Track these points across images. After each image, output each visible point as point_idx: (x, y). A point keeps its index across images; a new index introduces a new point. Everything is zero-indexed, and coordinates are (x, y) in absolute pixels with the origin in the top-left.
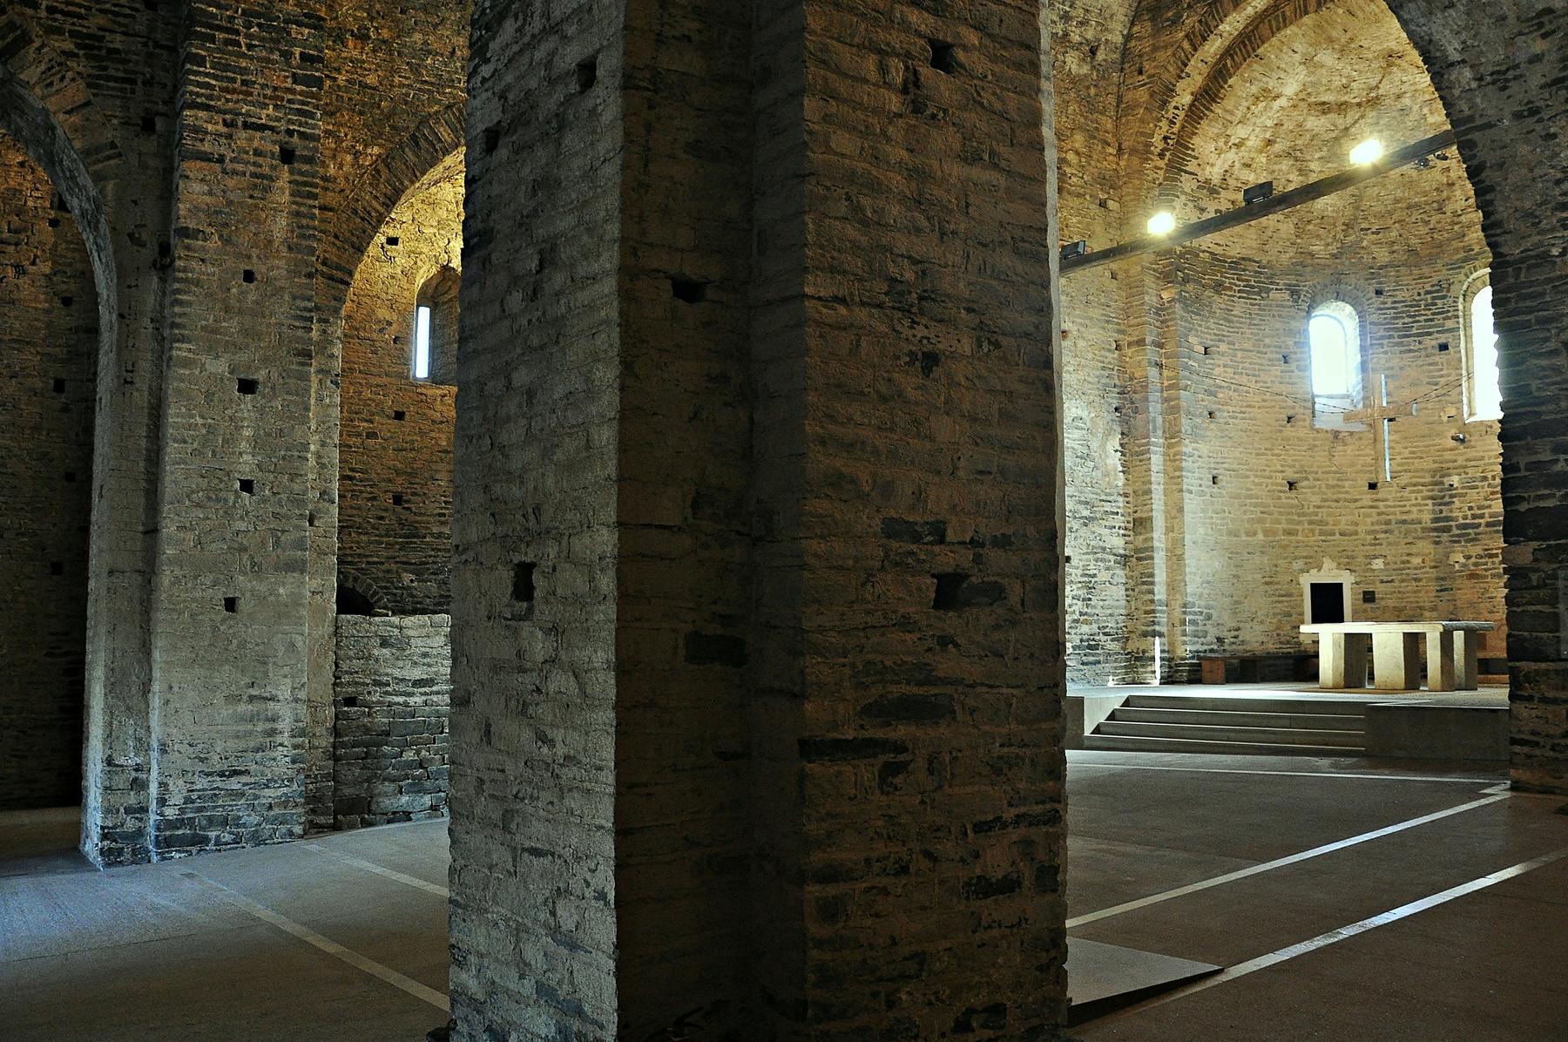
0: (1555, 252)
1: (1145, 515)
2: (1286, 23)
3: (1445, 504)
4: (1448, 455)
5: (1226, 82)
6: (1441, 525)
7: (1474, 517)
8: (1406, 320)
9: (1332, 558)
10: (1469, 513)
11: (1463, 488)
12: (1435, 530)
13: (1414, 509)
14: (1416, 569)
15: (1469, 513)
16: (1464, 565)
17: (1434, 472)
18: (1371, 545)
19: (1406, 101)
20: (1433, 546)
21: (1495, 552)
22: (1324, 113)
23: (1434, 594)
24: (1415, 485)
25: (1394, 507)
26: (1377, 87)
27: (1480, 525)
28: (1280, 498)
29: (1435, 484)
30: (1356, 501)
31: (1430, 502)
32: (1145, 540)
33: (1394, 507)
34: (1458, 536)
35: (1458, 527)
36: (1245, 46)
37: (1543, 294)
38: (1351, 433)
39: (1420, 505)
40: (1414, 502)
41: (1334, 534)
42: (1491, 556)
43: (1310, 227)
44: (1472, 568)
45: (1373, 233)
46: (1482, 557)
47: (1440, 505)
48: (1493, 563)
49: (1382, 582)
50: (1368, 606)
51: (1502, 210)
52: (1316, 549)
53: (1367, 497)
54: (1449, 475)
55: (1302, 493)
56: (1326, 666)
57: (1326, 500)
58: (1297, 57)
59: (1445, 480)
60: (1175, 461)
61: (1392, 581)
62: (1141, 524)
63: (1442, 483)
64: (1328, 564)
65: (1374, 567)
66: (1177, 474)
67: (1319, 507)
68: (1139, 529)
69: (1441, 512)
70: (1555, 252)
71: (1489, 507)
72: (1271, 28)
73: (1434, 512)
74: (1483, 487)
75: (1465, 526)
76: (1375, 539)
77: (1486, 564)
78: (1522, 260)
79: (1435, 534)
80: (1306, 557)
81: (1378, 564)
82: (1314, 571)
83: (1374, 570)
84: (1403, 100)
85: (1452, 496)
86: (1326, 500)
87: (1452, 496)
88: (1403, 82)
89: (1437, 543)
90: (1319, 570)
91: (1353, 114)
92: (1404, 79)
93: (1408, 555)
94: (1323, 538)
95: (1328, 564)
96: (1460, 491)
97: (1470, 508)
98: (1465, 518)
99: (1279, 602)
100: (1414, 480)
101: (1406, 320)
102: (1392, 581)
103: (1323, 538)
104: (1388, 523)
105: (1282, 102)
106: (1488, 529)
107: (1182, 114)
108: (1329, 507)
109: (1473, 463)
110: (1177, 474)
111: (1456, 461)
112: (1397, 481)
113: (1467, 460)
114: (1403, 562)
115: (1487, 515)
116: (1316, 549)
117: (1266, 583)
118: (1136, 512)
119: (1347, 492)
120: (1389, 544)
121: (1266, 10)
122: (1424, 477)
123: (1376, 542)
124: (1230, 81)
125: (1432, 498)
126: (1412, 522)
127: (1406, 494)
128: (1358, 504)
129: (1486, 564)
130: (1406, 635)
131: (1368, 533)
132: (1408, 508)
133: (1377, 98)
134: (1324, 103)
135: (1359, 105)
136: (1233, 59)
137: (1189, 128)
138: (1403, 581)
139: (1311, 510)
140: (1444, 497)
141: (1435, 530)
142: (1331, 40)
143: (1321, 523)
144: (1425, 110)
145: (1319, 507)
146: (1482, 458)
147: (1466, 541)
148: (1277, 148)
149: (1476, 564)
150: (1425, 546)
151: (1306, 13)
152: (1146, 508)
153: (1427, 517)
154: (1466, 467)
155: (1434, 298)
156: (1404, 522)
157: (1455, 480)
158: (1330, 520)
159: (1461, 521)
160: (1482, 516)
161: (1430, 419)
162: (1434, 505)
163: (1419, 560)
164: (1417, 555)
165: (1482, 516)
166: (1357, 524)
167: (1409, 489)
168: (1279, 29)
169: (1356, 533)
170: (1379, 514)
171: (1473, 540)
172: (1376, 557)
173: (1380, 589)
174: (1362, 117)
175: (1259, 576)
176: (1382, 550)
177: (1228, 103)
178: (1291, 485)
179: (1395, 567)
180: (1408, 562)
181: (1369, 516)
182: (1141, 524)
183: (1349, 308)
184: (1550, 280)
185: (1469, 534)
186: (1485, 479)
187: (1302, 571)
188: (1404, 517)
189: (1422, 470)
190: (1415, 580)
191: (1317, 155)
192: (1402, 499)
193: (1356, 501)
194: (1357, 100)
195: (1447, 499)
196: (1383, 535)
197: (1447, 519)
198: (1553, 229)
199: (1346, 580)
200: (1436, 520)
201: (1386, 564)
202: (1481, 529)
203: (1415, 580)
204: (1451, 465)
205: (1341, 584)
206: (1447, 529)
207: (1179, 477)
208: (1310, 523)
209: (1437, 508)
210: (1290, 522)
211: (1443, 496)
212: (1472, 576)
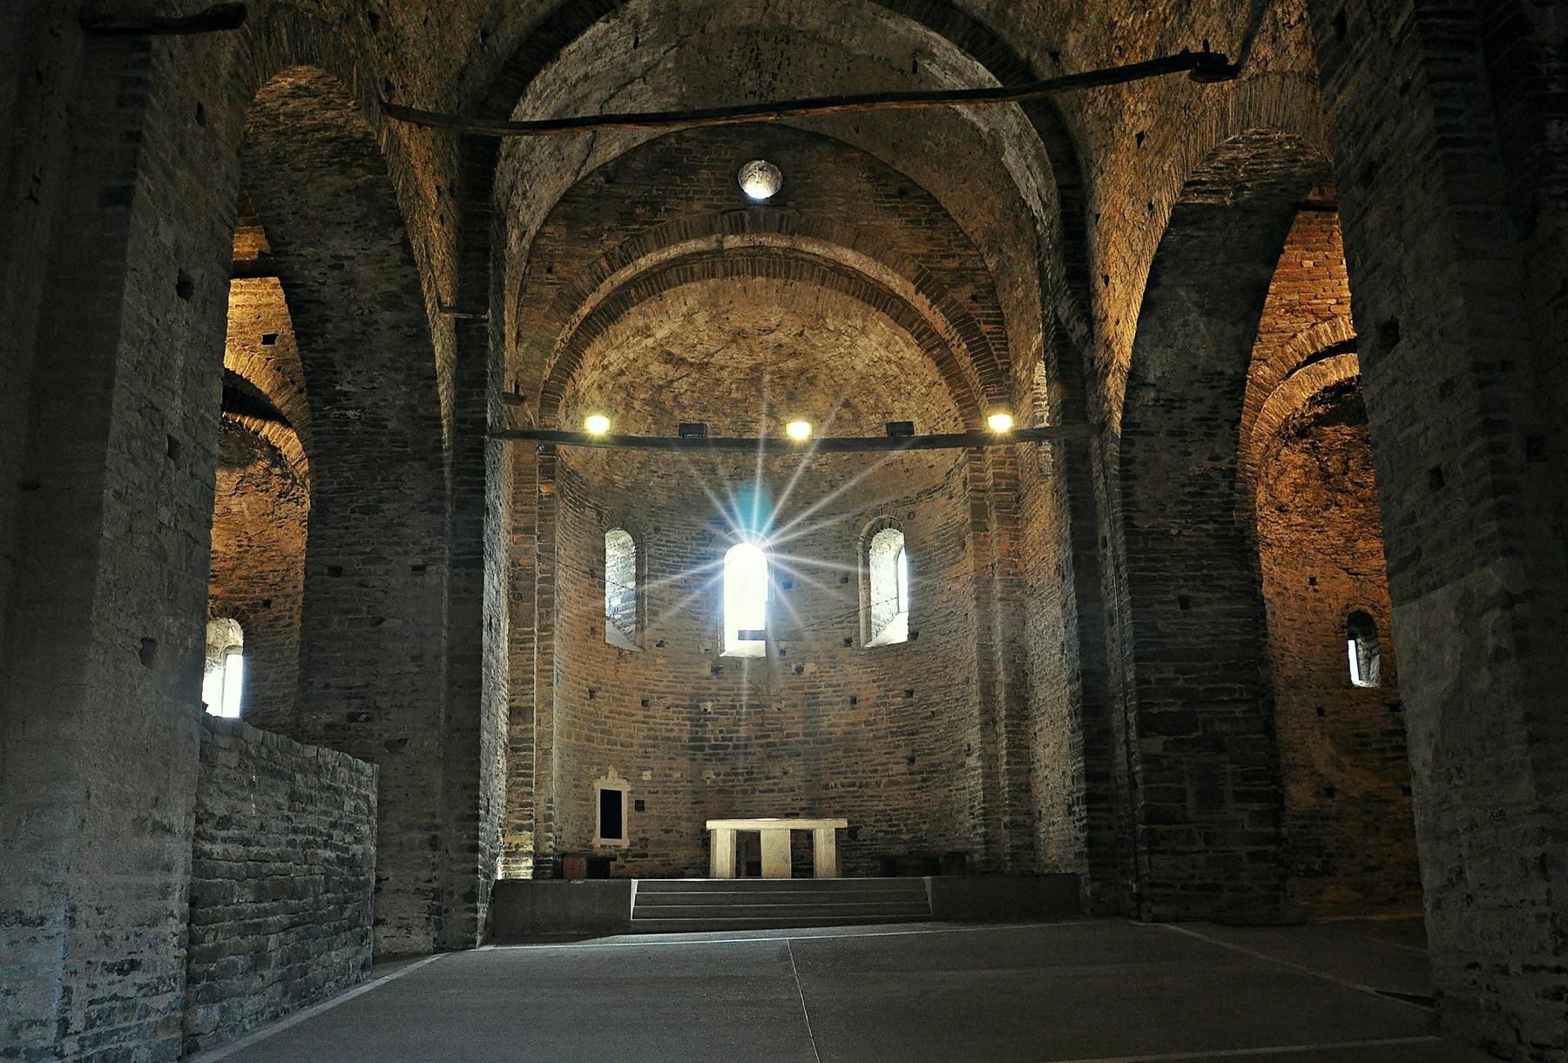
0: (1173, 532)
1: (523, 705)
2: (692, 277)
3: (701, 726)
4: (704, 683)
5: (627, 309)
6: (697, 744)
7: (724, 739)
8: (676, 559)
9: (616, 767)
10: (720, 736)
11: (715, 713)
12: (692, 748)
13: (676, 728)
14: (676, 782)
15: (720, 736)
16: (714, 782)
17: (692, 697)
18: (642, 757)
19: (725, 374)
20: (687, 762)
22: (666, 362)
23: (689, 805)
26: (712, 356)
27: (728, 747)
28: (584, 705)
29: (692, 707)
30: (633, 715)
31: (688, 723)
32: (522, 731)
33: (661, 724)
34: (709, 755)
35: (710, 747)
36: (651, 284)
37: (1164, 560)
38: (631, 652)
39: (678, 724)
40: (676, 722)
43: (617, 458)
44: (721, 784)
45: (659, 477)
46: (729, 775)
49: (649, 792)
51: (1139, 495)
52: (605, 757)
53: (640, 714)
54: (704, 701)
55: (597, 702)
56: (724, 859)
58: (684, 309)
59: (701, 704)
60: (545, 654)
62: (520, 713)
63: (698, 707)
64: (612, 772)
65: (644, 778)
66: (548, 667)
67: (608, 717)
68: (517, 719)
69: (697, 733)
70: (1173, 532)
72: (679, 277)
73: (691, 732)
75: (716, 747)
76: (646, 752)
78: (1150, 533)
81: (647, 776)
83: (643, 781)
84: (722, 372)
85: (706, 720)
87: (706, 720)
88: (732, 358)
89: (693, 760)
91: (683, 371)
92: (735, 356)
95: (612, 772)
96: (712, 716)
97: (721, 732)
101: (676, 559)
102: (657, 792)
104: (656, 738)
105: (650, 342)
107: (578, 322)
108: (614, 718)
110: (548, 667)
114: (666, 776)
116: (605, 757)
117: (576, 786)
118: (513, 701)
119: (626, 706)
120: (656, 758)
121: (672, 260)
122: (684, 701)
123: (646, 756)
124: (632, 310)
125: (690, 719)
126: (675, 739)
127: (670, 714)
128: (634, 718)
130: (795, 833)
131: (641, 746)
133: (707, 364)
134: (670, 354)
135: (692, 364)
136: (637, 290)
137: (583, 338)
138: (665, 793)
139: (603, 719)
141: (692, 748)
142: (715, 305)
143: (609, 732)
144: (734, 386)
145: (608, 717)
147: (719, 760)
148: (624, 380)
149: (723, 781)
150: (684, 762)
151: (714, 276)
152: (524, 698)
153: (686, 736)
155: (698, 545)
156: (668, 739)
157: (709, 705)
158: (614, 731)
160: (731, 739)
161: (692, 650)
162: (692, 726)
163: (678, 775)
164: (677, 769)
165: (731, 739)
166: (632, 738)
168: (686, 281)
170: (650, 729)
171: (723, 759)
173: (648, 799)
174: (687, 375)
176: (651, 762)
177: (620, 327)
178: (592, 693)
179: (660, 779)
180: (670, 776)
181: (640, 730)
182: (520, 713)
183: (626, 537)
184: (1168, 551)
185: (719, 754)
189: (683, 694)
190: (676, 792)
191: (642, 396)
192: (667, 718)
194: (693, 360)
196: (651, 750)
198: (1175, 517)
199: (624, 788)
200: (693, 739)
202: (729, 750)
203: (676, 792)
204: (705, 692)
205: (620, 792)
206: (701, 748)
207: (549, 671)
208: (602, 732)
210: (590, 729)
211: (698, 719)
212: (720, 791)
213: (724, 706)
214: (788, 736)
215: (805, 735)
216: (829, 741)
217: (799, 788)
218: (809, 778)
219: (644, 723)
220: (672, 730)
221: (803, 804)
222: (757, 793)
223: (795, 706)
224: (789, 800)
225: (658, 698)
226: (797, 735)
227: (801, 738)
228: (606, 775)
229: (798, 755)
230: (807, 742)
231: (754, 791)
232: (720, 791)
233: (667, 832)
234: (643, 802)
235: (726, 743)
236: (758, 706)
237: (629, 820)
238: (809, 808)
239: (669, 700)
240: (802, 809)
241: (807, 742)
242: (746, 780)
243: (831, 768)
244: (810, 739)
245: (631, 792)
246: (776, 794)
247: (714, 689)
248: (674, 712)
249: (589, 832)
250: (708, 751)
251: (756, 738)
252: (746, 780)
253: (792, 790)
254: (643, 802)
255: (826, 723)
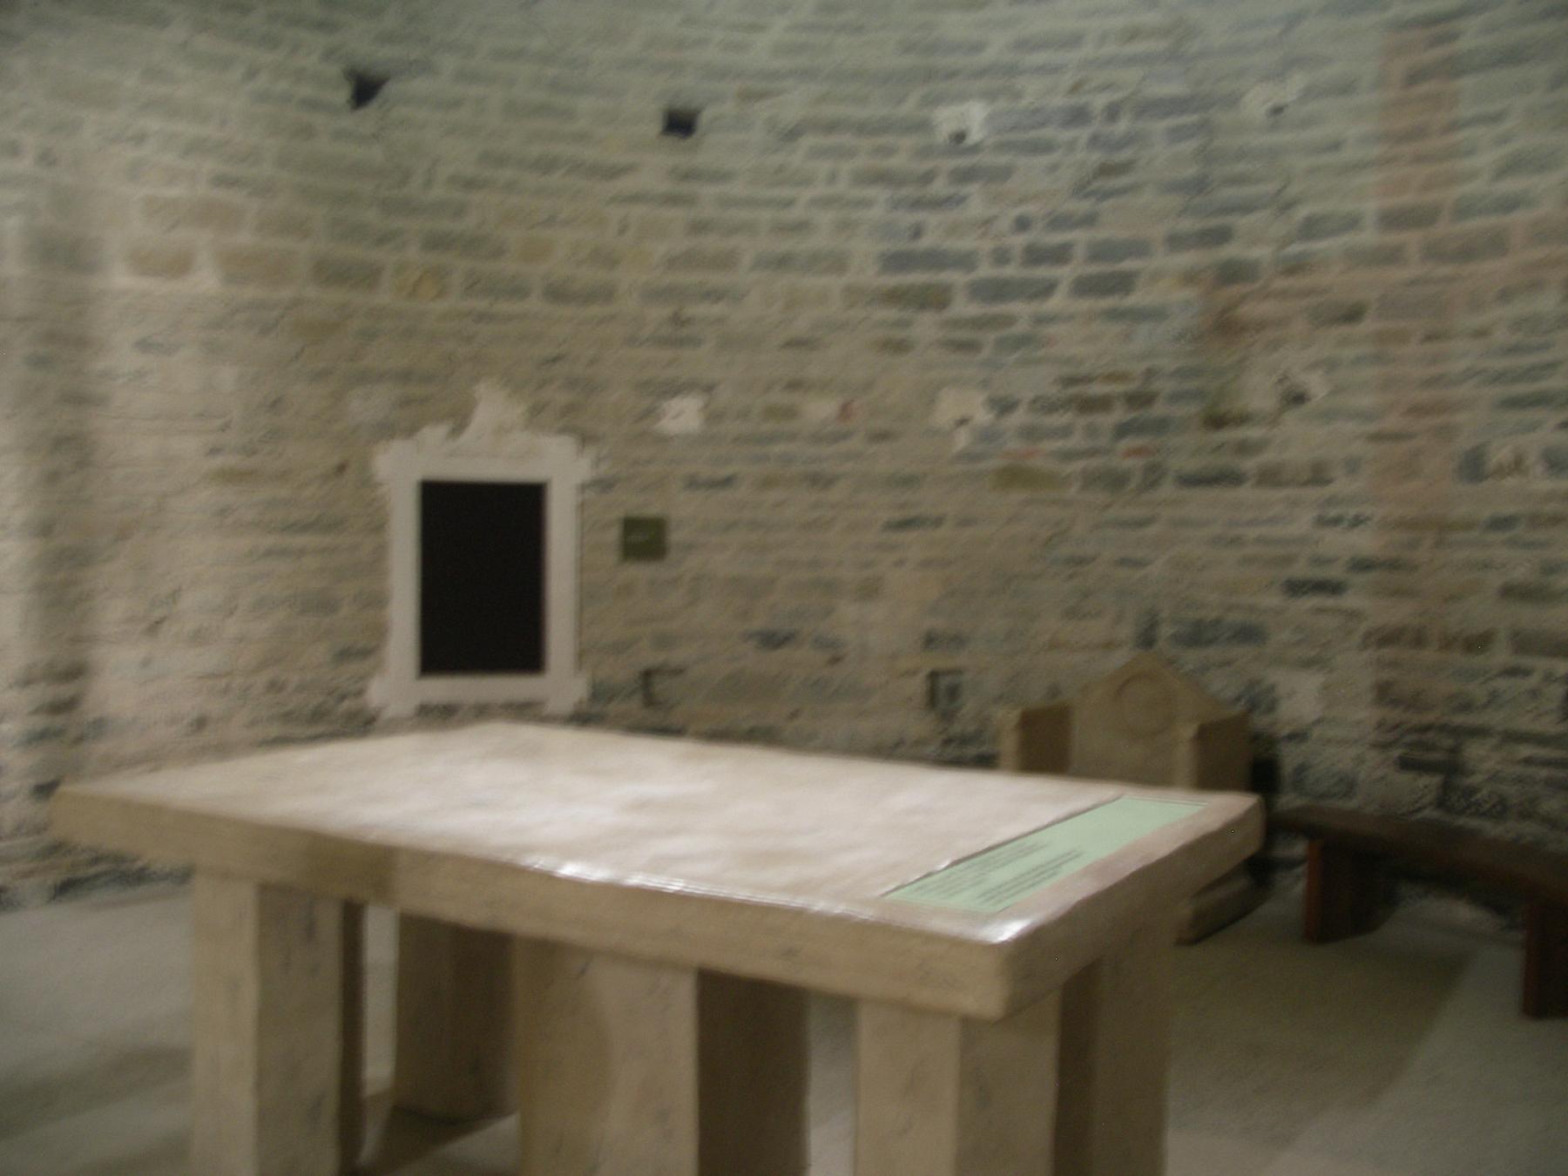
3: (938, 204)
7: (1035, 256)
11: (1003, 147)
12: (894, 297)
13: (825, 218)
14: (817, 438)
15: (1019, 241)
21: (1097, 389)
24: (832, 127)
25: (751, 203)
30: (613, 173)
33: (751, 203)
40: (820, 190)
41: (518, 291)
42: (1089, 405)
47: (917, 204)
48: (1091, 431)
49: (693, 483)
50: (640, 572)
54: (961, 97)
57: (501, 161)
61: (727, 482)
63: (923, 126)
69: (917, 232)
71: (1089, 220)
74: (1071, 146)
75: (996, 291)
76: (677, 320)
77: (1065, 432)
79: (891, 313)
80: (405, 376)
82: (434, 434)
83: (663, 440)
86: (501, 161)
90: (458, 429)
93: (794, 385)
94: (481, 304)
96: (986, 159)
97: (1022, 224)
98: (1001, 257)
99: (283, 553)
100: (831, 111)
102: (727, 482)
103: (481, 304)
106: (1086, 304)
109: (1040, 58)
111: (977, 47)
112: (762, 110)
113: (1023, 45)
114: (772, 412)
115: (1079, 252)
119: (582, 138)
128: (626, 184)
129: (1065, 432)
132: (796, 213)
138: (768, 483)
139: (438, 192)
140: (927, 178)
141: (894, 297)
143: (471, 245)
145: (470, 184)
146: (1074, 40)
147: (1001, 344)
153: (864, 250)
154: (1012, 71)
156: (783, 262)
159: (985, 271)
160: (1059, 255)
162: (896, 205)
165: (1059, 255)
167: (808, 141)
169: (606, 294)
172: (675, 389)
175: (188, 446)
180: (790, 413)
185: (1008, 321)
186: (1078, 116)
187: (387, 431)
188: (786, 245)
193: (613, 173)
195: (939, 188)
197: (936, 260)
201: (713, 416)
202: (1056, 303)
203: (819, 481)
206: (934, 299)
208: (436, 242)
209: (908, 218)
212: (1013, 476)
213: (1039, 117)
214: (1312, 228)
215: (1393, 220)
216: (1496, 244)
217: (1353, 466)
218: (1392, 423)
219: (672, 200)
220: (801, 227)
221: (1365, 542)
222: (1167, 490)
223: (1345, 88)
224: (1302, 524)
225: (748, 97)
226: (1352, 223)
227: (1368, 237)
228: (459, 419)
229: (1353, 314)
230: (1391, 257)
231: (1153, 475)
232: (1013, 476)
233: (772, 640)
234: (631, 525)
235: (1042, 272)
236: (1176, 105)
237: (586, 595)
238: (1394, 565)
239: (794, 104)
240: (1362, 565)
241: (1391, 257)
242: (1122, 431)
243: (1499, 378)
244: (1411, 239)
245: (603, 485)
246: (1245, 492)
247: (997, 48)
248: (818, 153)
249: (344, 655)
250: (963, 307)
251: (1176, 242)
252: (1122, 431)
253: (1318, 475)
254: (631, 525)
255: (1487, 158)
